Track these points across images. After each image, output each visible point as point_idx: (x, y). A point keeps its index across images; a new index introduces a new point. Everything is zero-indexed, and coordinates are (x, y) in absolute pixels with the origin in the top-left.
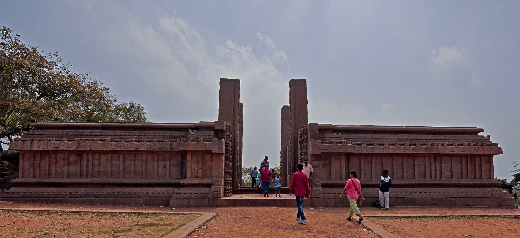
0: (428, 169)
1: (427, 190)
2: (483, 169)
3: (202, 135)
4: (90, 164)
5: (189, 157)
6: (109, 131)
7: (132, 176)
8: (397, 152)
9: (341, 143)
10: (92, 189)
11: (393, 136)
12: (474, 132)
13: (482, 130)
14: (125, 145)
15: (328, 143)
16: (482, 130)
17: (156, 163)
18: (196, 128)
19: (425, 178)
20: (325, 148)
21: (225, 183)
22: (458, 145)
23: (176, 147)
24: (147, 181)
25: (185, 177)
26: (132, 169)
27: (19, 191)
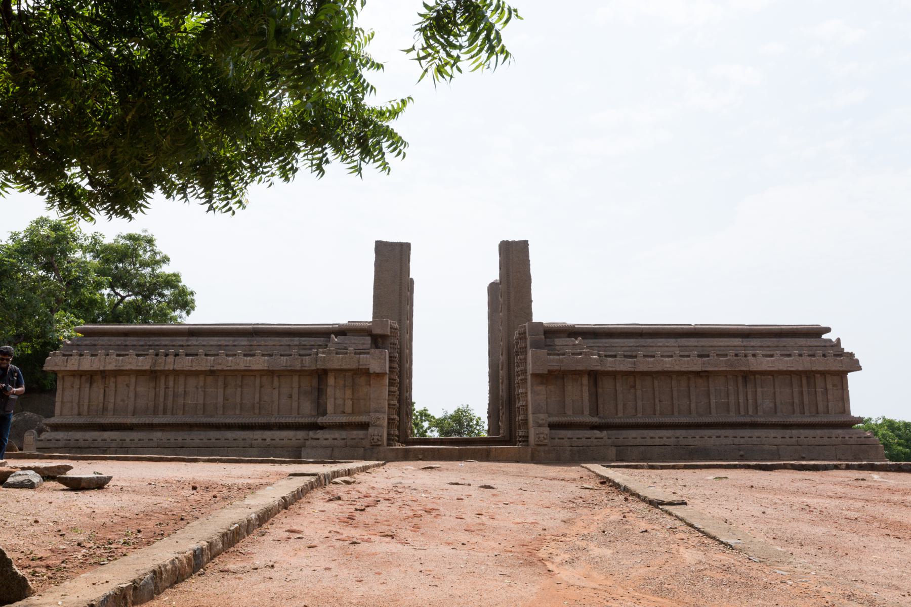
0: (732, 399)
1: (730, 432)
2: (830, 397)
3: (353, 343)
4: (171, 393)
5: (331, 381)
7: (238, 412)
8: (677, 368)
9: (581, 354)
11: (672, 342)
12: (816, 332)
13: (828, 330)
14: (228, 361)
15: (558, 355)
16: (828, 330)
17: (276, 392)
18: (342, 331)
19: (728, 411)
20: (554, 362)
21: (389, 423)
22: (782, 355)
23: (308, 363)
24: (262, 420)
25: (324, 413)
26: (238, 400)
27: (58, 437)
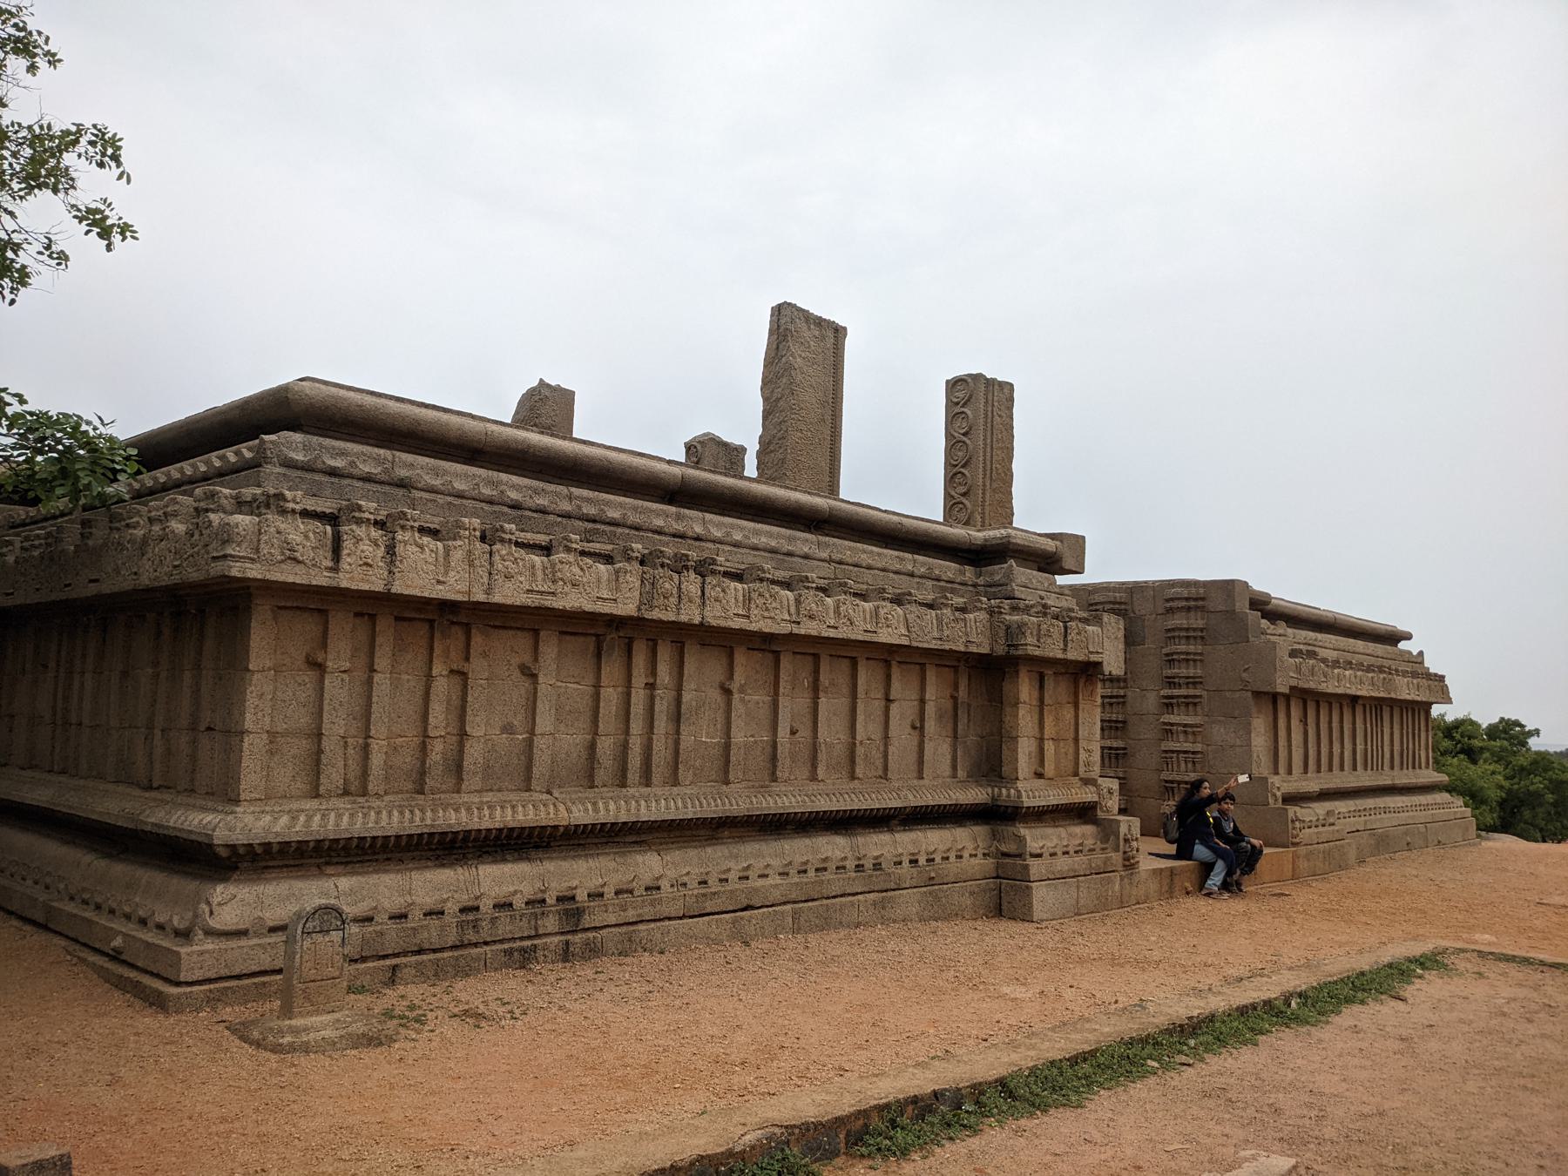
4: (662, 707)
5: (1025, 689)
6: (708, 516)
12: (1392, 638)
13: (1408, 637)
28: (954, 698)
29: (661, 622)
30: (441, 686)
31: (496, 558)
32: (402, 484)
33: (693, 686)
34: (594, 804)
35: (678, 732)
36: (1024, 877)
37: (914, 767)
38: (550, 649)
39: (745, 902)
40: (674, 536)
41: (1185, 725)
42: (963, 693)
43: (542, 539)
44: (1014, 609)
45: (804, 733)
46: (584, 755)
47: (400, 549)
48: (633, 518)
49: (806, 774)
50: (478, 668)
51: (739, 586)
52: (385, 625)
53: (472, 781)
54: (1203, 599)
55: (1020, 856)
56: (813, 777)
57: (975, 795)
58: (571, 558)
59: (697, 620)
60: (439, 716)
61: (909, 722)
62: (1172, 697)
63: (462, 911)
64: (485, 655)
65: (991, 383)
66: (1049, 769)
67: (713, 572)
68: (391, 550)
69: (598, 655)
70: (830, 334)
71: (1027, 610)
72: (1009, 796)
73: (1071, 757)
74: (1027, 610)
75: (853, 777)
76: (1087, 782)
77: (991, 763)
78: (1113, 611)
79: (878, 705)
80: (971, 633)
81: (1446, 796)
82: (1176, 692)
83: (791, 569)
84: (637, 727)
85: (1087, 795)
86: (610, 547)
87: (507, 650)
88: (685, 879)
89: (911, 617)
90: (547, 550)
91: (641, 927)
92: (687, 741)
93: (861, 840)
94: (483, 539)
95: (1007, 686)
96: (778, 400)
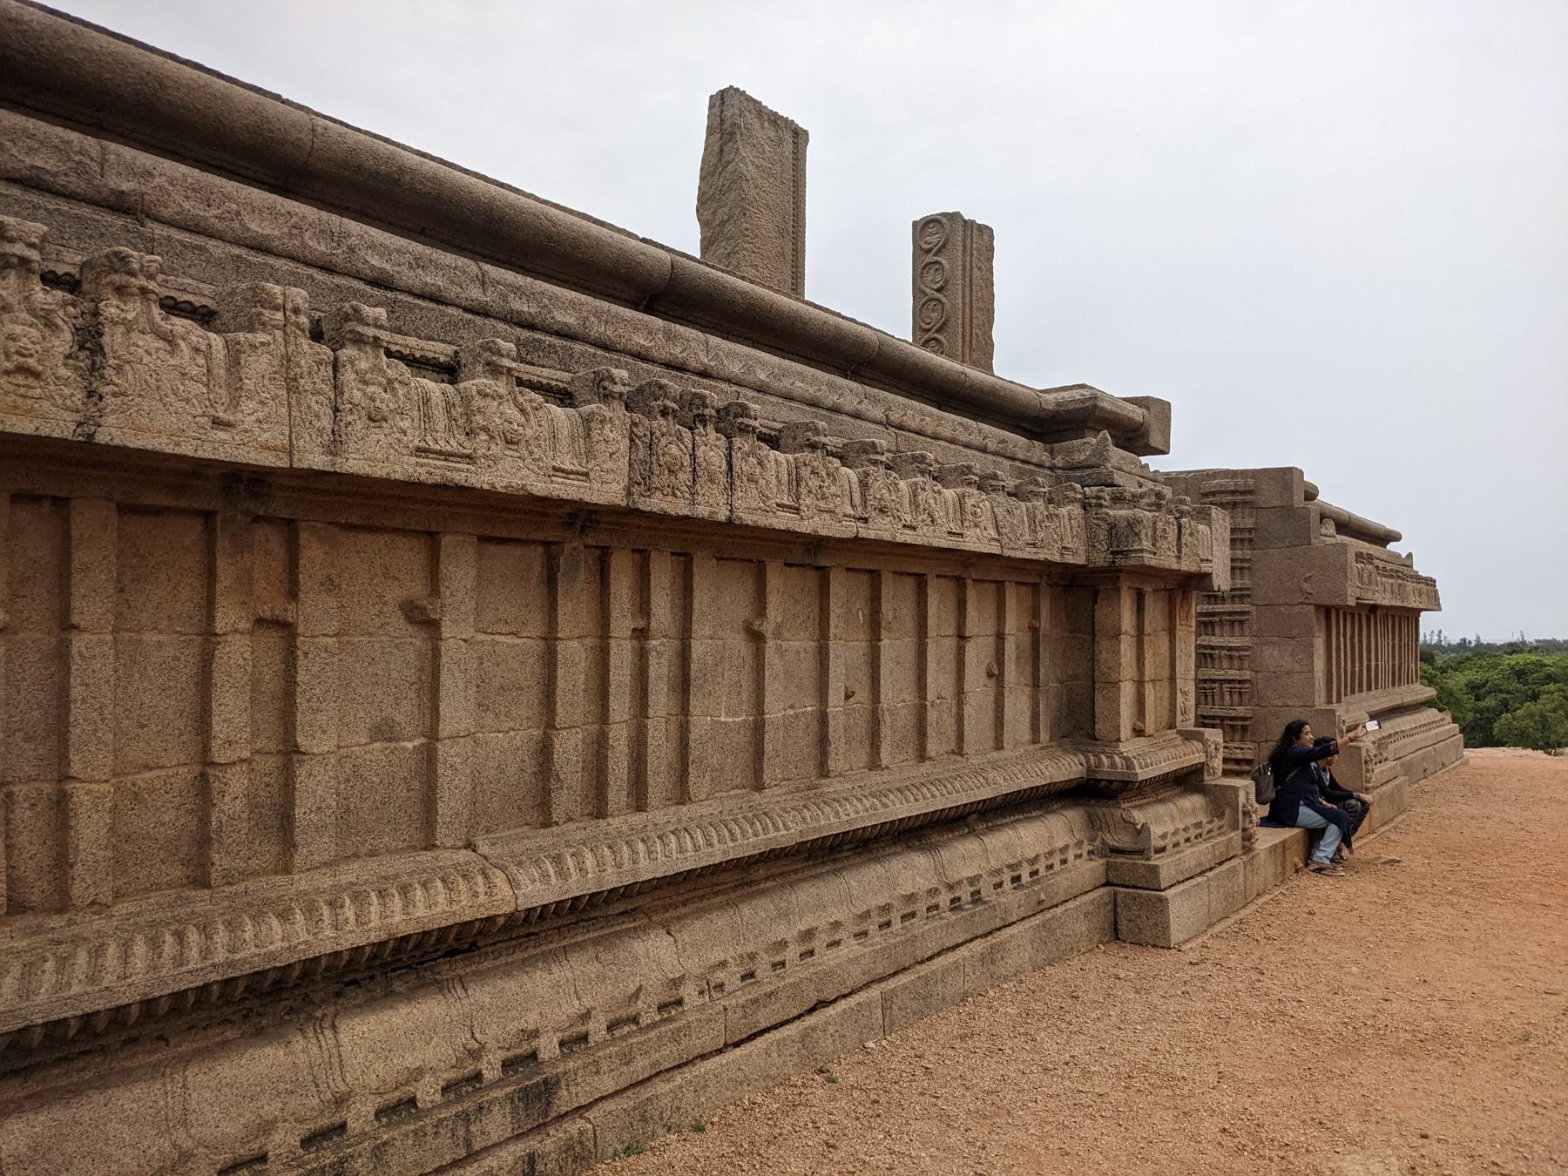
4: (660, 669)
10: (721, 921)
12: (1383, 538)
13: (1397, 538)
16: (1396, 537)
28: (1034, 630)
29: (663, 517)
30: (239, 653)
31: (348, 376)
32: (120, 205)
33: (707, 631)
34: (557, 860)
35: (685, 710)
36: (1150, 881)
37: (990, 734)
38: (461, 570)
39: (814, 998)
40: (668, 365)
41: (1230, 649)
42: (1044, 624)
43: (440, 350)
44: (1118, 499)
45: (862, 695)
46: (530, 766)
47: (113, 339)
48: (598, 329)
49: (862, 757)
50: (316, 614)
51: (781, 457)
52: (93, 524)
53: (314, 846)
54: (1251, 492)
55: (1141, 852)
56: (874, 764)
57: (1066, 768)
58: (501, 386)
59: (722, 515)
60: (232, 715)
61: (984, 666)
62: (1212, 614)
63: (308, 1142)
64: (330, 585)
65: (969, 225)
66: (1150, 726)
67: (744, 430)
68: (89, 339)
69: (551, 582)
70: (788, 138)
71: (1135, 500)
72: (1113, 765)
73: (1166, 703)
74: (1135, 500)
75: (922, 756)
76: (1187, 736)
77: (1079, 721)
78: (1222, 505)
79: (950, 644)
80: (1060, 536)
81: (1432, 714)
82: (1218, 608)
83: (840, 434)
84: (621, 707)
85: (1191, 756)
86: (566, 376)
87: (380, 572)
88: (721, 975)
89: (1000, 511)
90: (449, 371)
91: (661, 1087)
92: (700, 725)
93: (945, 854)
94: (317, 335)
95: (1101, 611)
96: (723, 223)
